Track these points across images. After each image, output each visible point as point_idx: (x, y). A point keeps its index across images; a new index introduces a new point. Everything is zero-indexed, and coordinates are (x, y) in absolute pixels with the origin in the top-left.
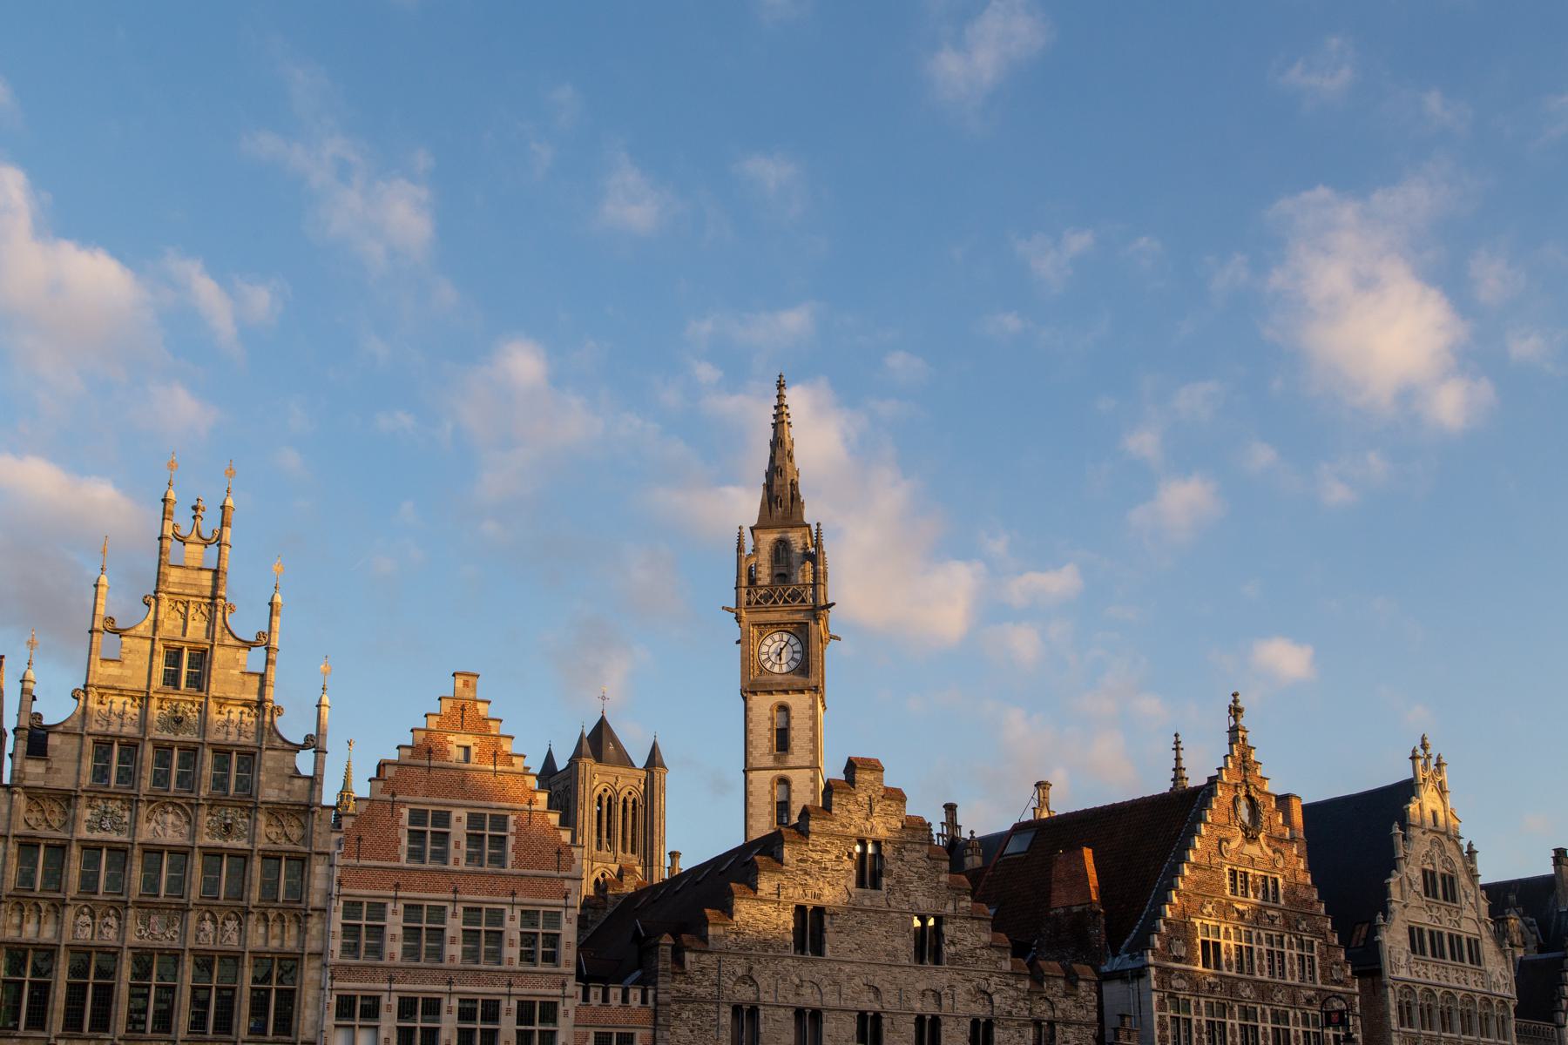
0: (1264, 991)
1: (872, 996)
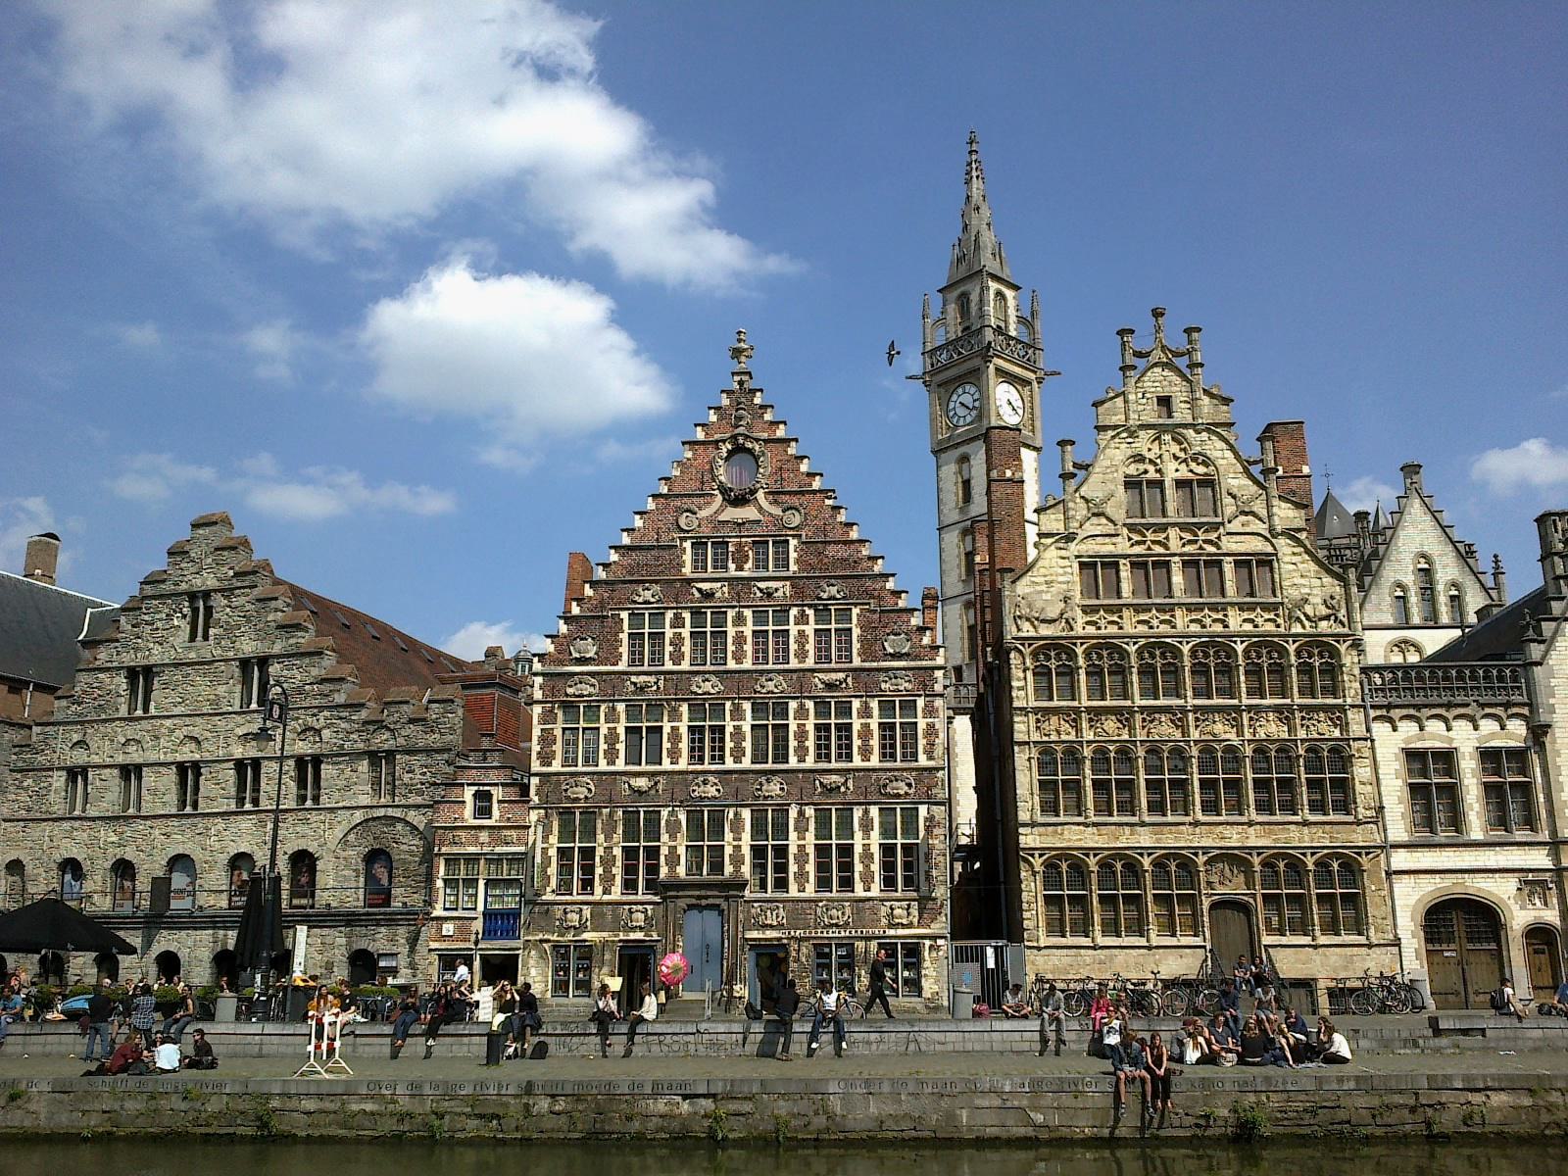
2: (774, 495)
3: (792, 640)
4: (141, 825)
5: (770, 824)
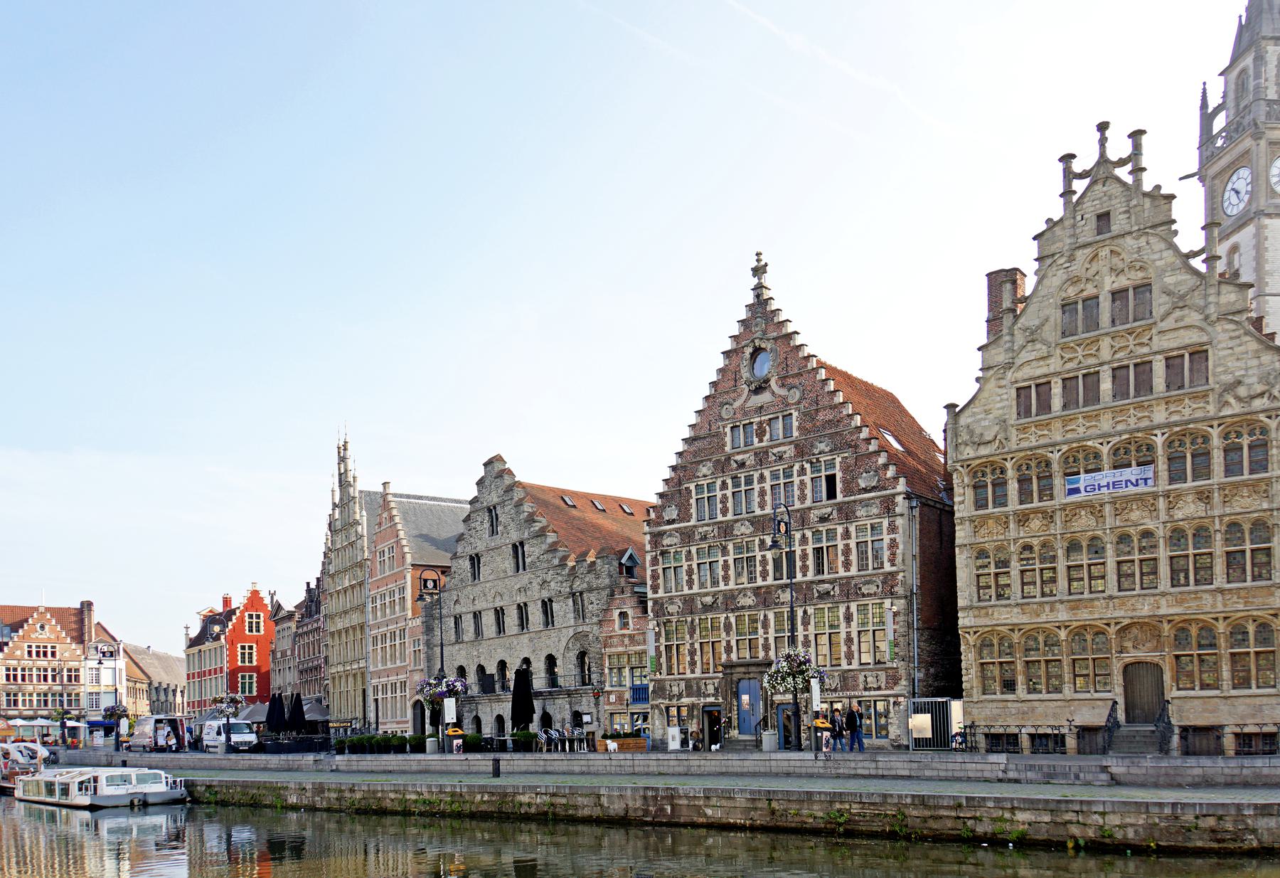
3: (796, 488)
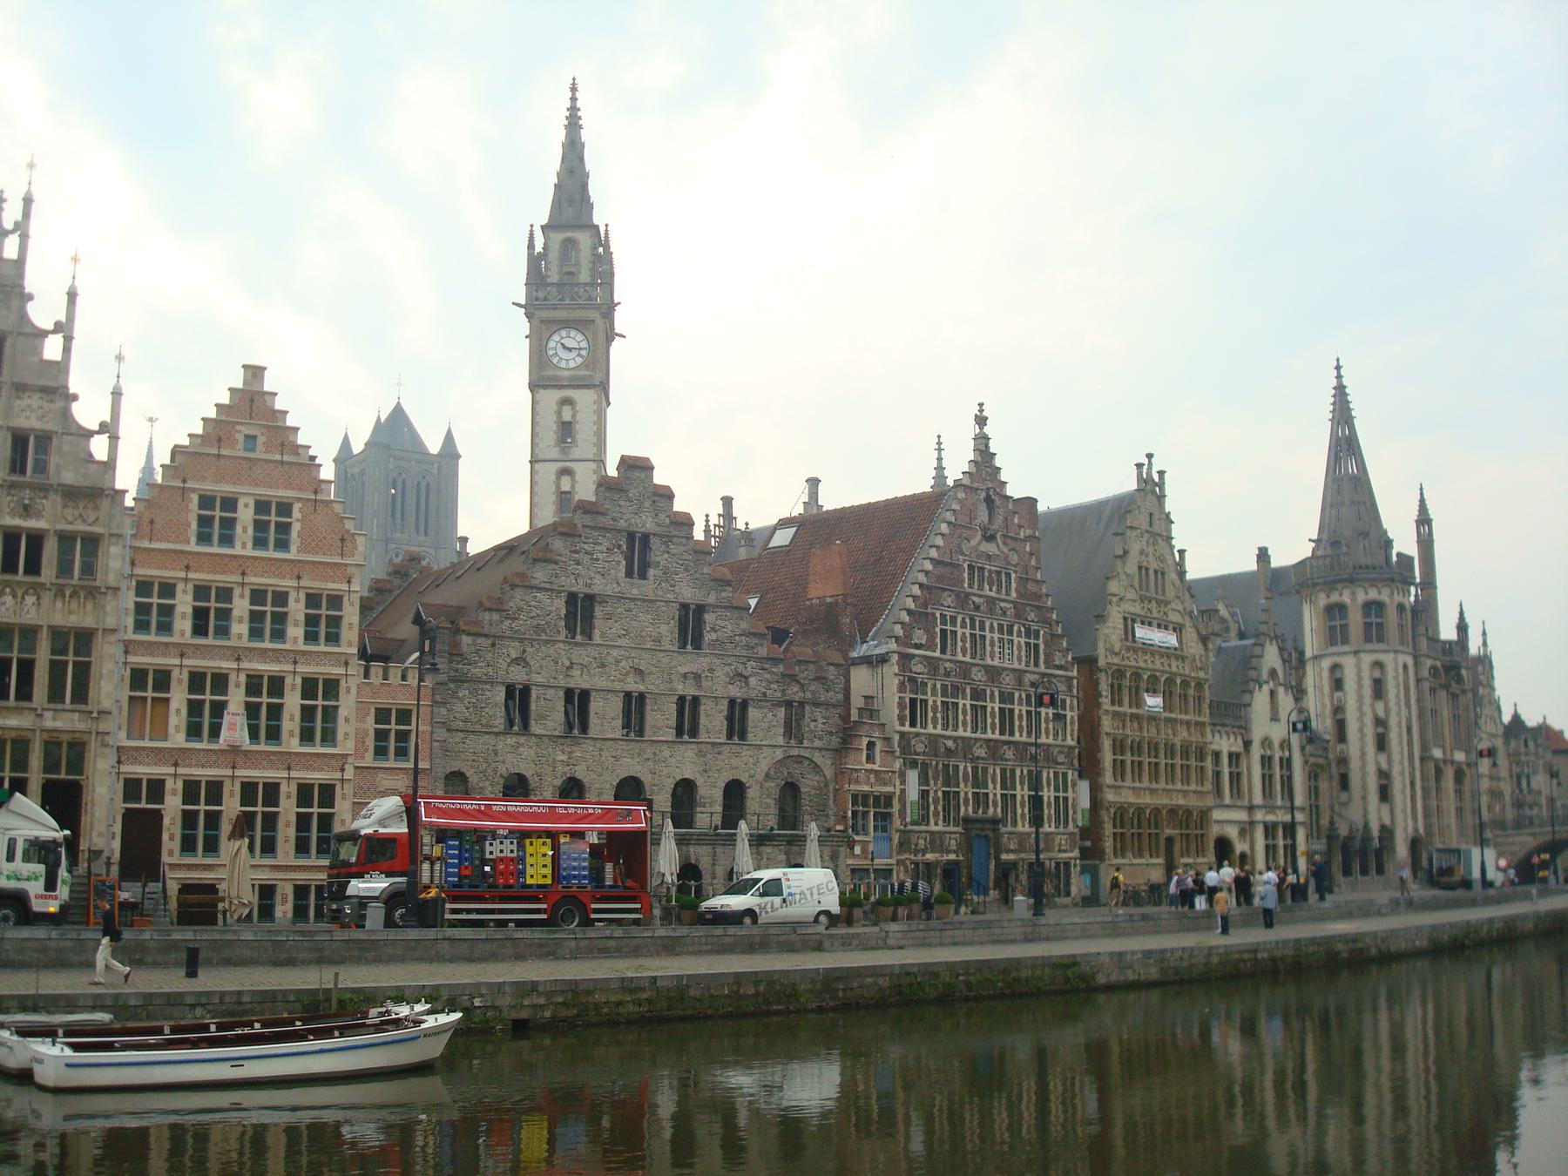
0: (993, 673)
1: (638, 679)
2: (1004, 536)
4: (588, 746)
5: (1007, 781)
